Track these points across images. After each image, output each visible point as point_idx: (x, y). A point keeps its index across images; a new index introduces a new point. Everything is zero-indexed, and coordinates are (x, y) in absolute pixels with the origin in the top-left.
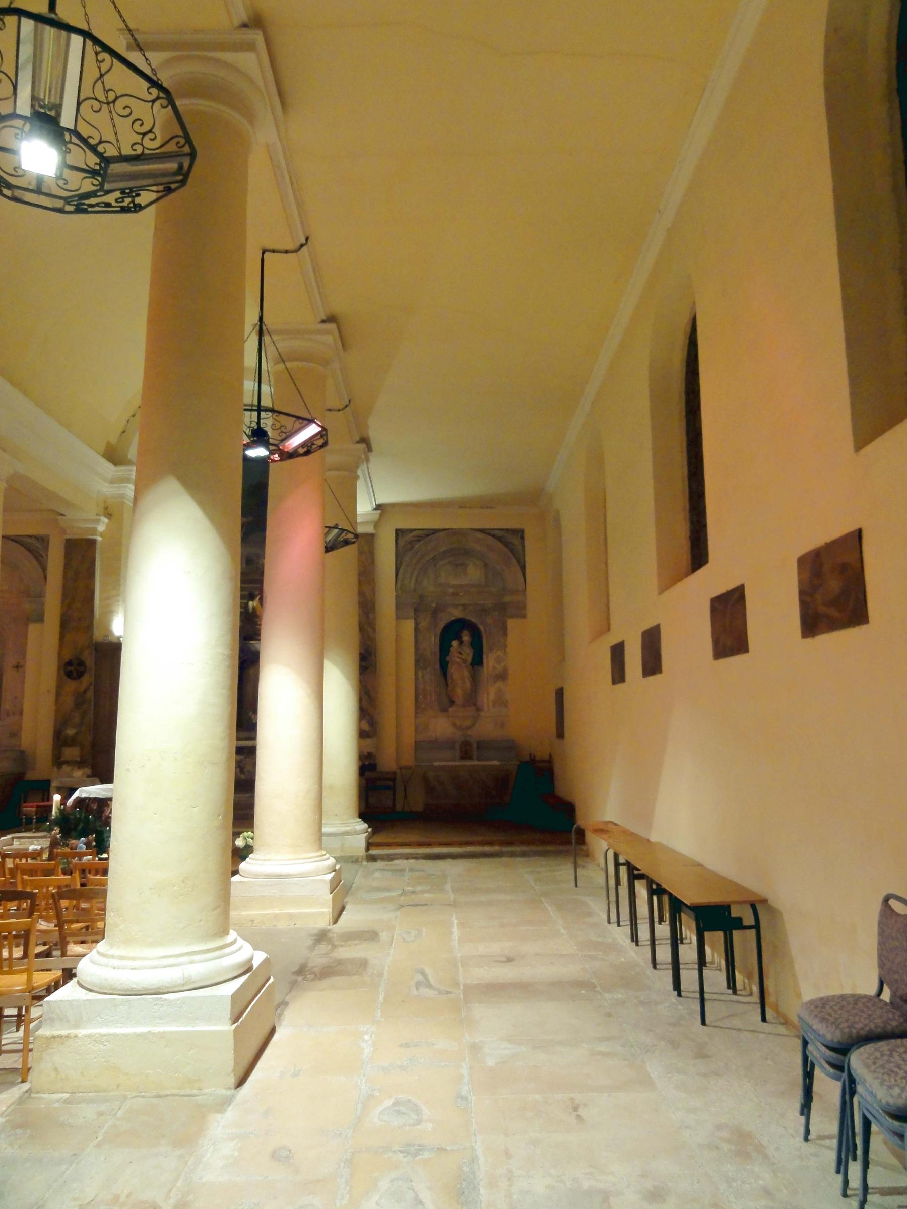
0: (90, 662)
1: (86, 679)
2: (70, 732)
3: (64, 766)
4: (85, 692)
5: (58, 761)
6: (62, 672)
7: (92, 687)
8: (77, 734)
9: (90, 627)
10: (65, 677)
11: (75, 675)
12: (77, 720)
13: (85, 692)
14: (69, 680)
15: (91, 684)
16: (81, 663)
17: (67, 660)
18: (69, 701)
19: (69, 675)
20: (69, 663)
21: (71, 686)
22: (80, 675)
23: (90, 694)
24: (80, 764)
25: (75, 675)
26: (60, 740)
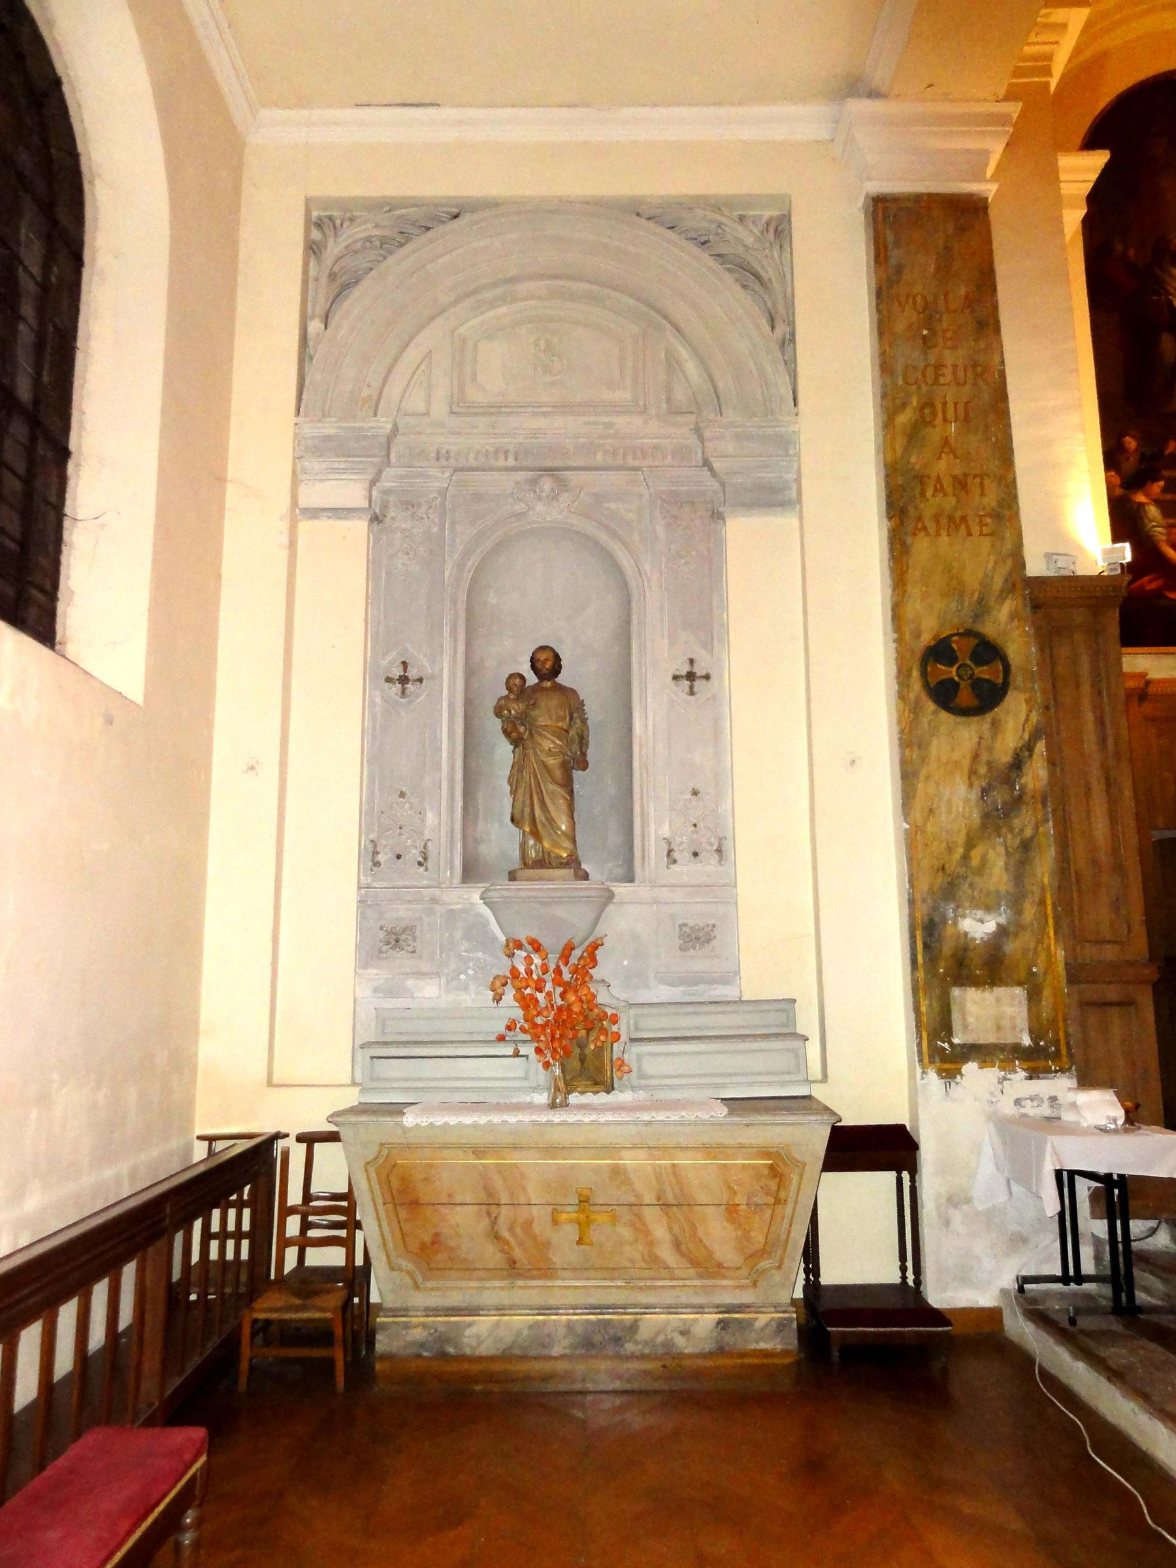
0: (1020, 647)
1: (1016, 716)
2: (978, 926)
3: (970, 1068)
4: (1017, 764)
5: (942, 1050)
6: (916, 685)
7: (1041, 747)
8: (1002, 931)
9: (1005, 513)
10: (931, 706)
11: (965, 697)
12: (998, 874)
13: (1017, 764)
14: (944, 715)
15: (1035, 736)
16: (988, 650)
17: (927, 638)
18: (958, 802)
19: (944, 696)
20: (939, 651)
21: (958, 738)
22: (988, 698)
23: (1036, 774)
24: (1036, 1059)
25: (965, 697)
26: (942, 966)
